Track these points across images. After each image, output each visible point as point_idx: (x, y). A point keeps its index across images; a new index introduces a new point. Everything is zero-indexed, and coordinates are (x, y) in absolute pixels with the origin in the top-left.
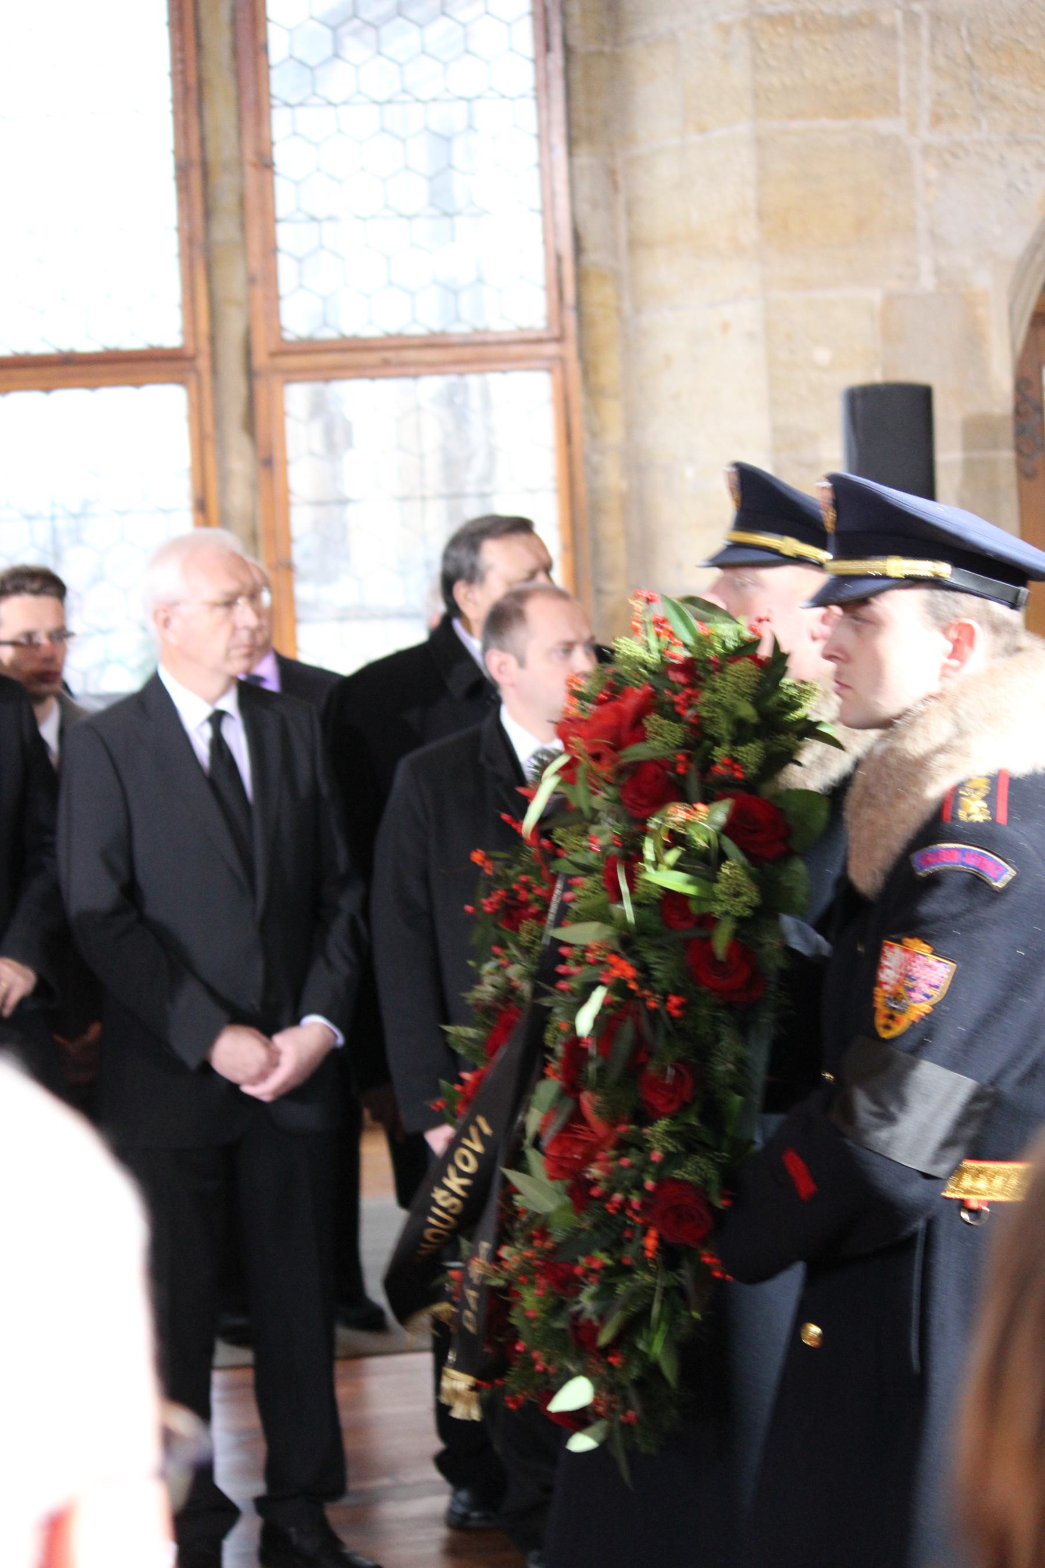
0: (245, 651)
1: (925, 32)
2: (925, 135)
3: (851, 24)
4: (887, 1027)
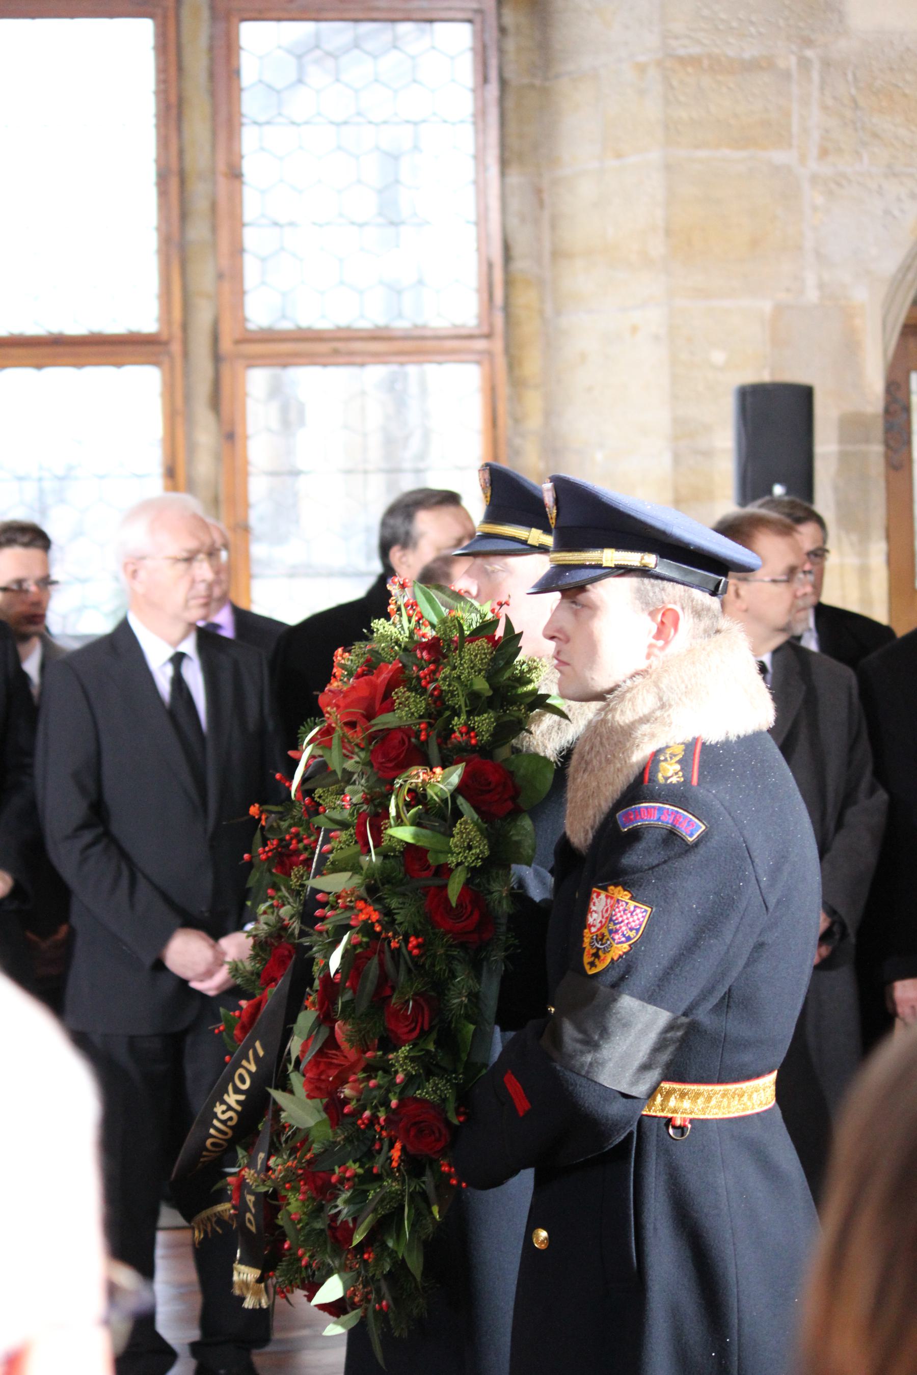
0: (202, 601)
1: (815, 76)
2: (813, 165)
4: (592, 964)
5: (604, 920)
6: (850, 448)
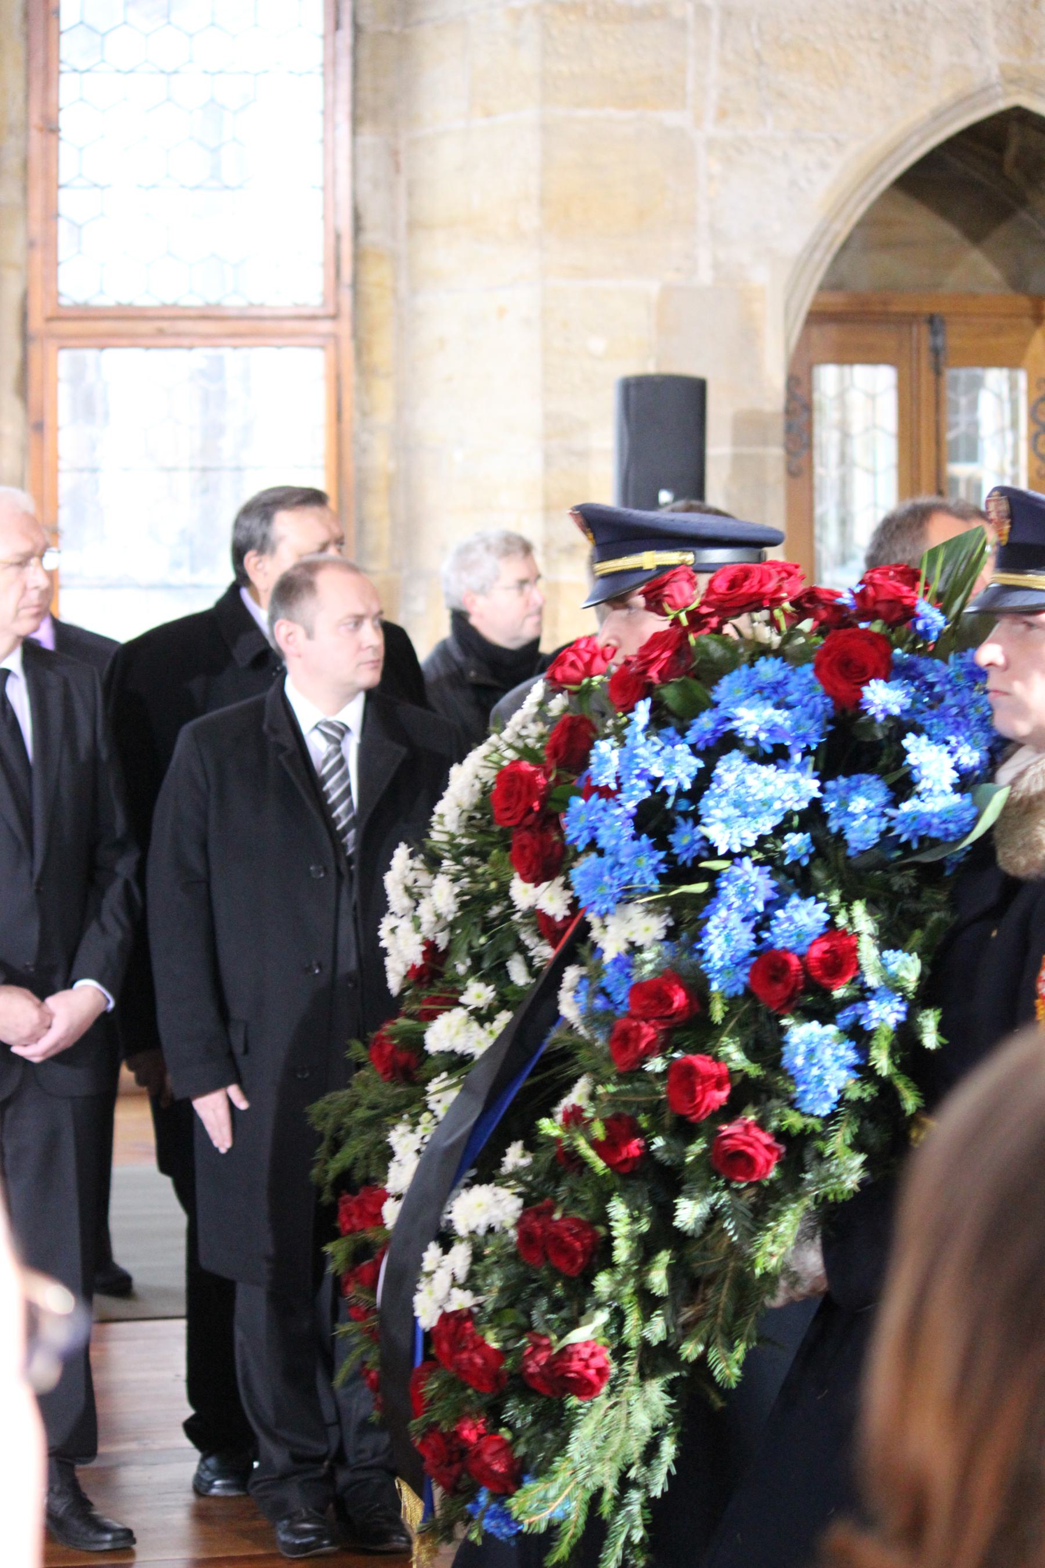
0: (34, 611)
1: (715, 26)
3: (643, 15)
6: (746, 450)
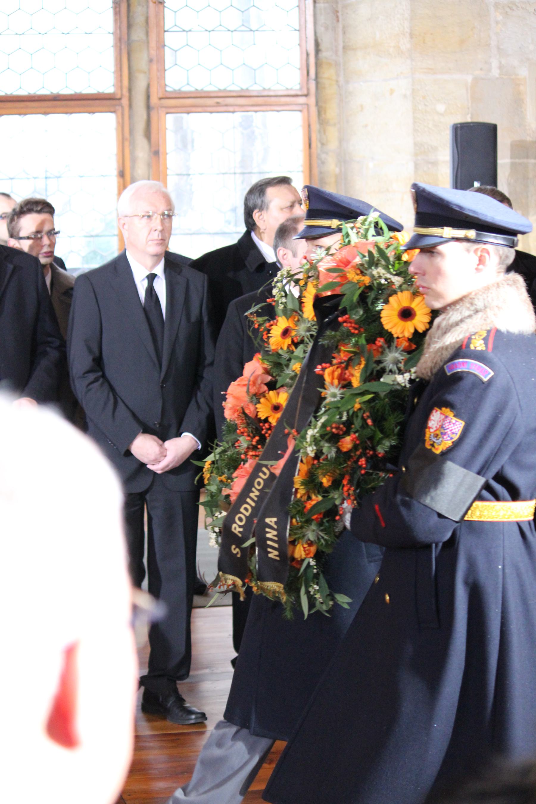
5: (438, 426)
